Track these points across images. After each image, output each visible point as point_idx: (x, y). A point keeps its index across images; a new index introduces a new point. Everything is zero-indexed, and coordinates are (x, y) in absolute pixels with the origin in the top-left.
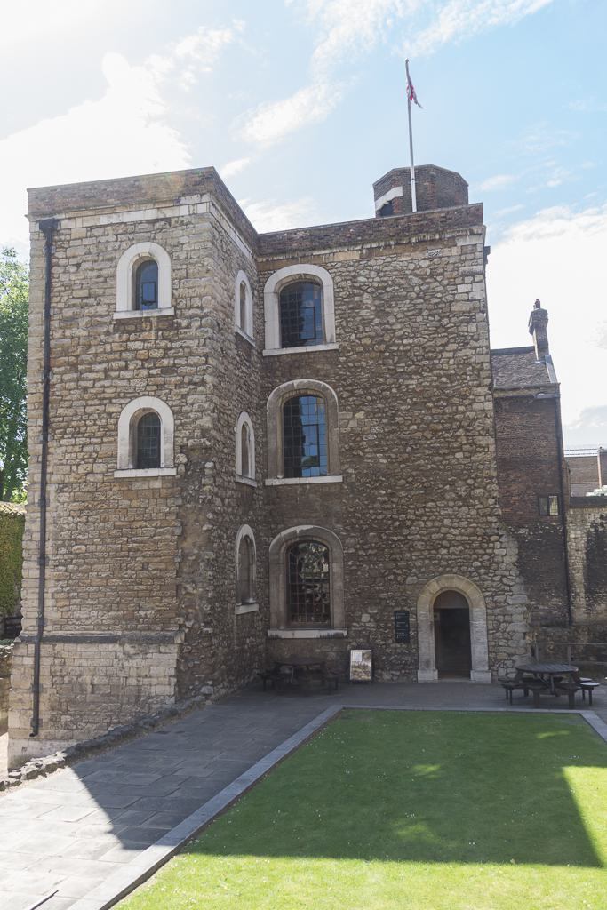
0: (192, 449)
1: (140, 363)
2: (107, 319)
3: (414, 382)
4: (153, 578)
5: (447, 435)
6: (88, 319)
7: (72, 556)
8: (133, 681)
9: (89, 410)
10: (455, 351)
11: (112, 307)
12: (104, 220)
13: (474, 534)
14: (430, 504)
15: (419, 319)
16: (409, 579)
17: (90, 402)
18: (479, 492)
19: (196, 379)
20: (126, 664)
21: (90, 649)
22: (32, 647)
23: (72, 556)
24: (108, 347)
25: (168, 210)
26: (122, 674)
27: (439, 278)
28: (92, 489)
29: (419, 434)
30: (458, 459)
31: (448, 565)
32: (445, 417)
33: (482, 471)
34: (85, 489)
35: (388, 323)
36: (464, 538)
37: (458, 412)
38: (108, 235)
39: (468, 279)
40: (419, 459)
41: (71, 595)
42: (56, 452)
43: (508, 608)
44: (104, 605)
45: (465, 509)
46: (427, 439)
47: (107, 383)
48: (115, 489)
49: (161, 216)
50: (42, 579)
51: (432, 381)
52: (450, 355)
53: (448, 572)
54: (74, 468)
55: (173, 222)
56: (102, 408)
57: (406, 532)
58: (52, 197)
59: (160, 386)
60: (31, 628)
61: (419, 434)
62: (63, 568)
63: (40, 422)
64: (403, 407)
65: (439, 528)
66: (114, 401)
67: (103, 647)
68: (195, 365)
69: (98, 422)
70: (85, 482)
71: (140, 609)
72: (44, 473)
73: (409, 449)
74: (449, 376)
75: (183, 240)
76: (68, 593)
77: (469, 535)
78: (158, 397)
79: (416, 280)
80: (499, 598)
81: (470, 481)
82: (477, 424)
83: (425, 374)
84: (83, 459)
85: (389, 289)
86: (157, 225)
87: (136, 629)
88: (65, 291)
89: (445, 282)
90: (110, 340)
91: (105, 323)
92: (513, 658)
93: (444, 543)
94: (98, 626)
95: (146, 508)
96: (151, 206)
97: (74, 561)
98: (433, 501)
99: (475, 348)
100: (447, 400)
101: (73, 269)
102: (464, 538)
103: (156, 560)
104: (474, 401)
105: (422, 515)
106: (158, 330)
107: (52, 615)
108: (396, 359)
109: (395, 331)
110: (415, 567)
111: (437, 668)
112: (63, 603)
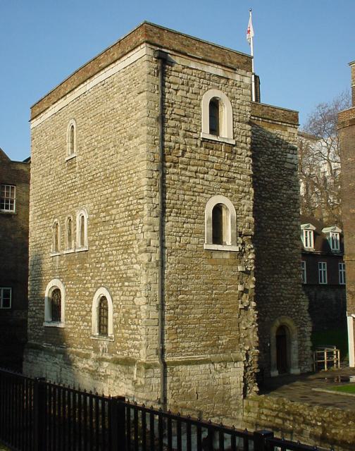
0: (245, 235)
1: (216, 172)
2: (195, 135)
3: (269, 204)
4: (225, 318)
5: (283, 237)
6: (184, 132)
7: (179, 303)
8: (220, 388)
9: (186, 197)
10: (286, 190)
11: (198, 126)
12: (193, 65)
13: (292, 294)
14: (276, 276)
15: (272, 167)
16: (266, 318)
17: (187, 193)
18: (295, 270)
19: (246, 189)
20: (217, 376)
21: (195, 369)
22: (158, 371)
23: (179, 303)
24: (198, 156)
25: (228, 73)
26: (215, 384)
27: (280, 147)
28: (191, 256)
29: (271, 235)
30: (287, 251)
31: (283, 311)
32: (283, 226)
33: (296, 259)
34: (186, 255)
35: (257, 166)
36: (289, 296)
37: (287, 225)
38: (195, 76)
39: (291, 151)
40: (271, 249)
41: (179, 330)
42: (168, 225)
43: (306, 334)
44: (199, 337)
45: (289, 279)
46: (275, 238)
47: (197, 181)
48: (204, 256)
49: (225, 76)
50: (163, 319)
51: (277, 205)
52: (284, 192)
53: (283, 315)
54: (178, 238)
55: (231, 82)
56: (194, 198)
57: (265, 291)
58: (162, 35)
59: (227, 190)
60: (152, 356)
61: (271, 235)
62: (173, 311)
63: (157, 201)
64: (265, 218)
65: (280, 289)
66: (201, 194)
67: (202, 366)
68: (244, 180)
69: (192, 208)
70: (185, 249)
71: (219, 339)
72: (163, 241)
73: (266, 243)
74: (283, 203)
75: (237, 96)
76: (177, 329)
77: (292, 294)
78: (227, 196)
79: (270, 145)
80: (302, 329)
81: (292, 264)
82: (294, 233)
83: (274, 201)
84: (183, 233)
85: (258, 146)
86: (223, 81)
87: (217, 353)
88: (169, 107)
89: (282, 150)
90: (199, 151)
91: (195, 138)
92: (308, 360)
93: (282, 298)
94: (196, 352)
95: (221, 271)
96: (220, 67)
97: (180, 306)
98: (277, 274)
99: (294, 190)
100: (282, 217)
101: (175, 92)
102: (289, 296)
103: (228, 306)
104: (293, 220)
105: (273, 282)
106: (226, 152)
107: (168, 346)
108: (261, 188)
109: (261, 171)
110: (269, 312)
111: (278, 369)
112: (173, 337)
